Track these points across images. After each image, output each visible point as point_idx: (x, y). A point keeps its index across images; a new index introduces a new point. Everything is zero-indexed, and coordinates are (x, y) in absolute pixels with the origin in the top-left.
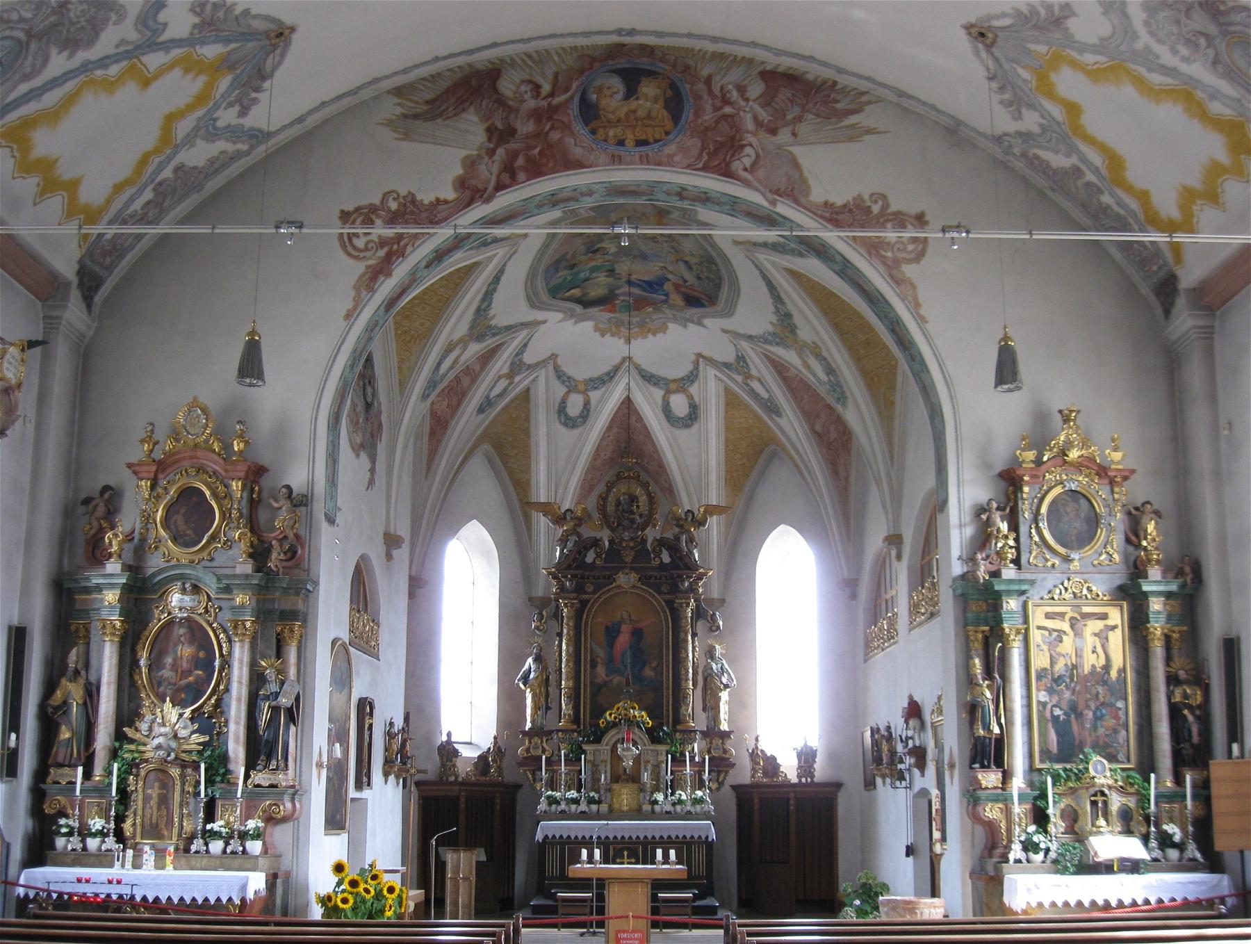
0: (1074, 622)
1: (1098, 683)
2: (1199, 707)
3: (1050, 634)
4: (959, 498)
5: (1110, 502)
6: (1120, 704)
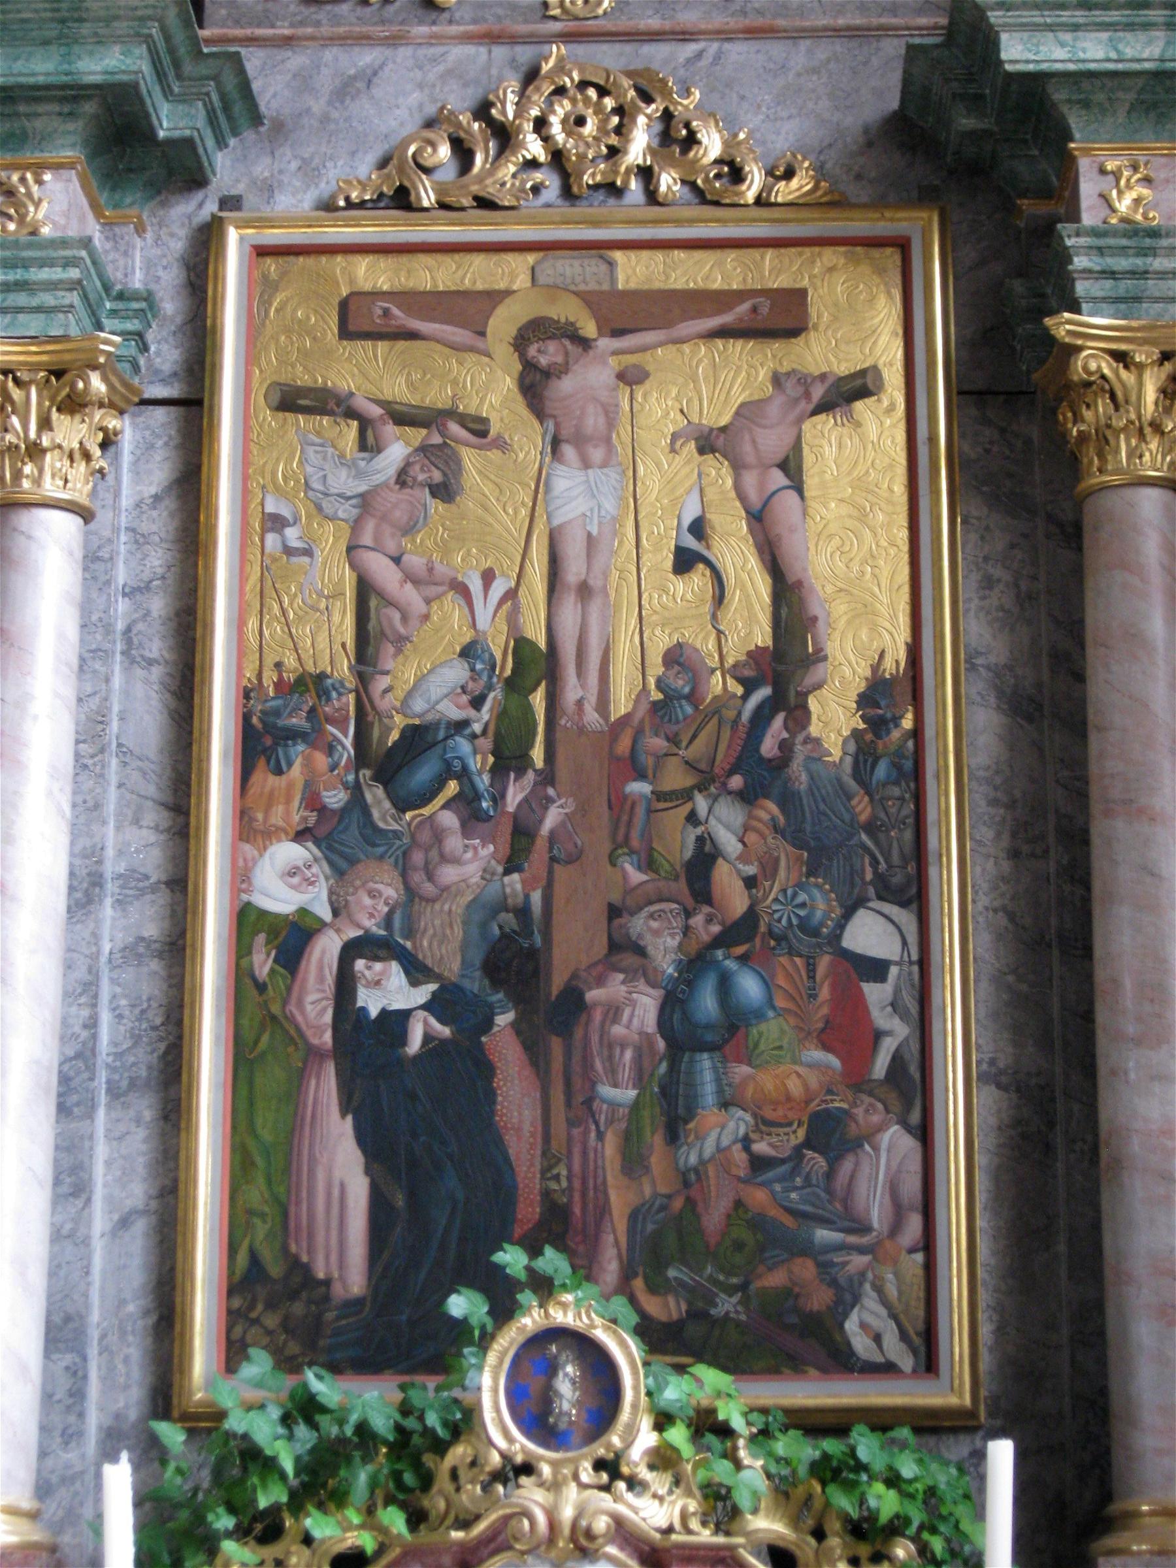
0: (548, 354)
3: (368, 444)
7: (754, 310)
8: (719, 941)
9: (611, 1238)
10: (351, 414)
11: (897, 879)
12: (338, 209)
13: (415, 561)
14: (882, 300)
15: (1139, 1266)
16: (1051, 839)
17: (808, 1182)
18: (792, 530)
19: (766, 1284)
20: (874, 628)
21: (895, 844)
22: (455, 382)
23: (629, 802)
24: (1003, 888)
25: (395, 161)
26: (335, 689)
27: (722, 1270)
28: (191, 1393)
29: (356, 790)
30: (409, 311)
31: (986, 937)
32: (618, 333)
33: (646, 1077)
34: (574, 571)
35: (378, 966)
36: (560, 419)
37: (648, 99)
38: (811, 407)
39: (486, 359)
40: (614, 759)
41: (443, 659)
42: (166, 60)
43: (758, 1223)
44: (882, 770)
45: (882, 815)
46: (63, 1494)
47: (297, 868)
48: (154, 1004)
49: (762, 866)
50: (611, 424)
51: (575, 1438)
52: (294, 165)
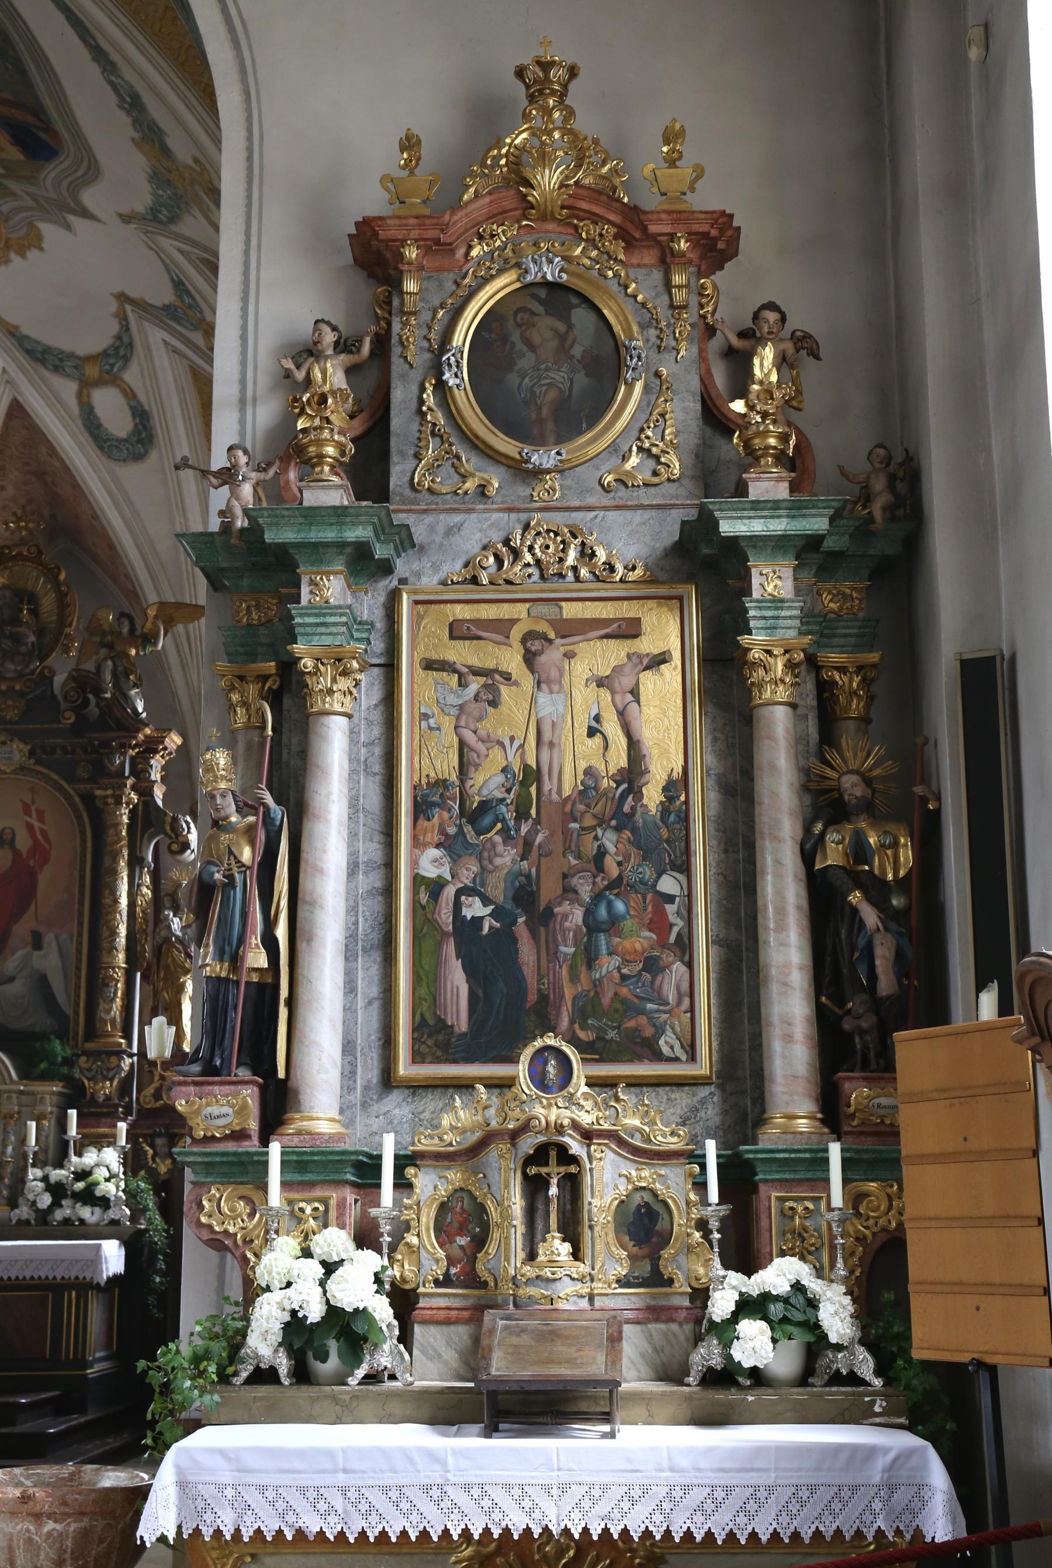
0: (535, 645)
1: (601, 822)
2: (902, 884)
3: (462, 684)
4: (244, 328)
5: (663, 313)
6: (668, 884)
7: (619, 626)
8: (607, 888)
10: (455, 671)
11: (679, 862)
14: (672, 621)
15: (775, 1019)
16: (741, 845)
17: (643, 985)
22: (497, 658)
27: (610, 1020)
29: (460, 827)
30: (478, 628)
31: (714, 885)
32: (563, 637)
34: (547, 736)
35: (470, 899)
37: (575, 537)
40: (564, 813)
42: (379, 529)
43: (624, 1001)
44: (672, 818)
46: (348, 1112)
49: (624, 858)
50: (561, 675)
51: (555, 1089)
52: (429, 565)
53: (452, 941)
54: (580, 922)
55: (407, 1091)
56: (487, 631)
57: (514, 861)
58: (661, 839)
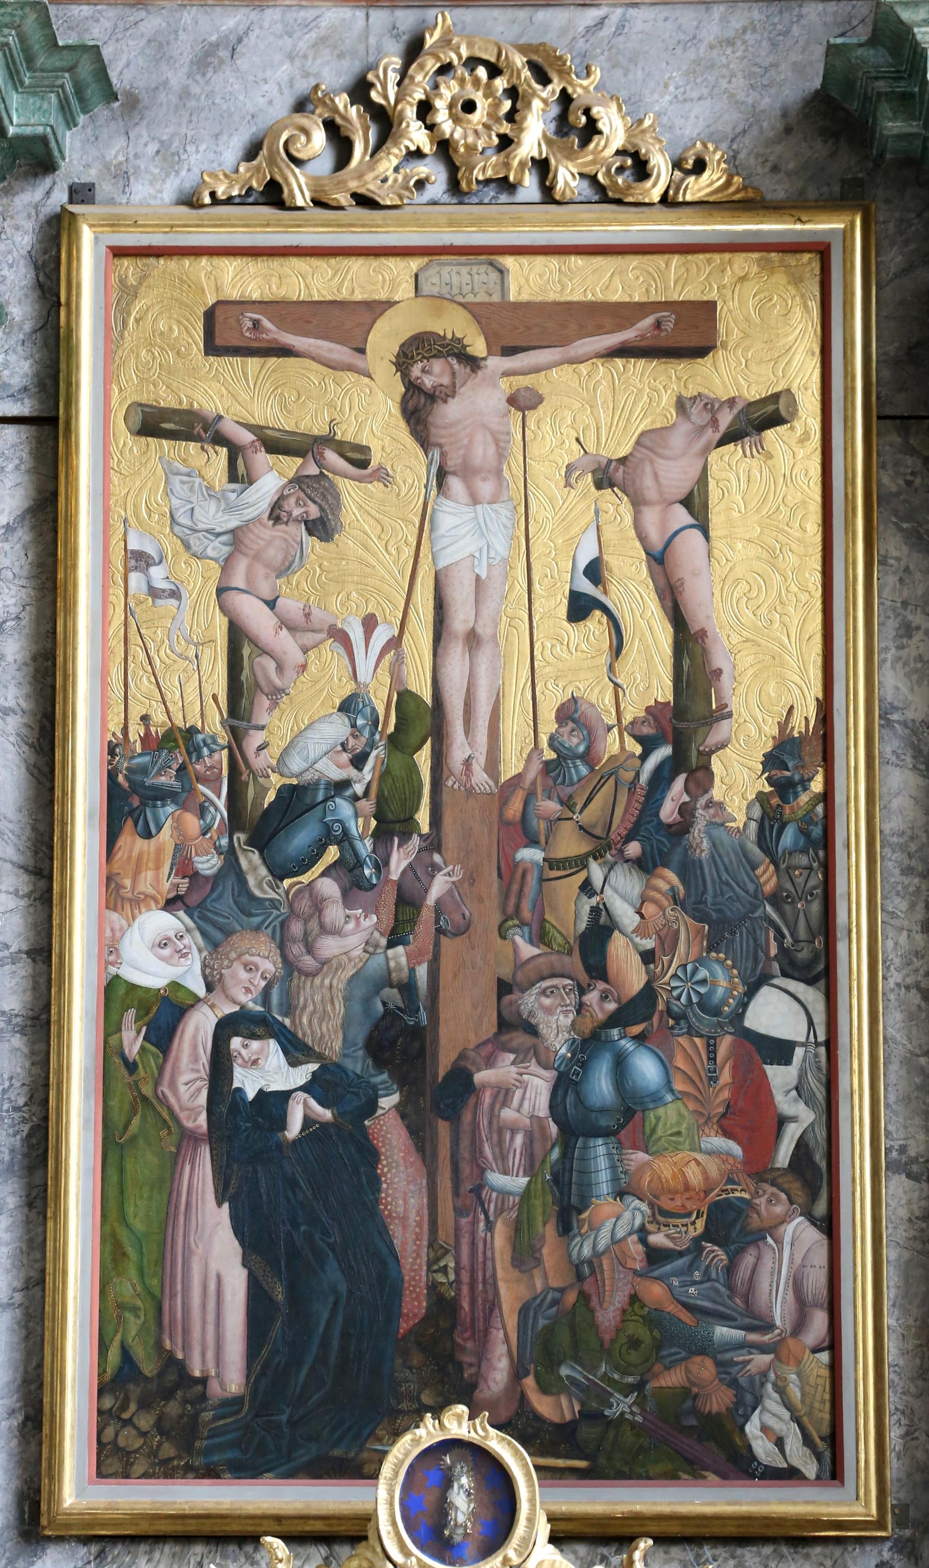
7: (658, 325)
8: (614, 1020)
9: (501, 1334)
10: (220, 439)
11: (804, 955)
12: (203, 206)
13: (290, 605)
14: (798, 312)
18: (696, 574)
19: (663, 1383)
20: (782, 681)
21: (802, 916)
22: (331, 405)
23: (520, 871)
24: (917, 963)
25: (265, 151)
26: (206, 745)
27: (617, 1368)
28: (60, 1501)
29: (230, 855)
30: (281, 324)
32: (509, 351)
33: (537, 1164)
35: (255, 1045)
36: (446, 448)
38: (718, 436)
39: (367, 380)
40: (504, 823)
41: (322, 713)
42: (19, 57)
44: (789, 837)
45: (789, 886)
47: (169, 939)
48: (17, 1084)
50: (502, 454)
51: (470, 1550)
52: (152, 148)
53: (205, 1154)
54: (543, 1110)
55: (82, 1551)
56: (306, 334)
57: (370, 947)
58: (757, 896)
